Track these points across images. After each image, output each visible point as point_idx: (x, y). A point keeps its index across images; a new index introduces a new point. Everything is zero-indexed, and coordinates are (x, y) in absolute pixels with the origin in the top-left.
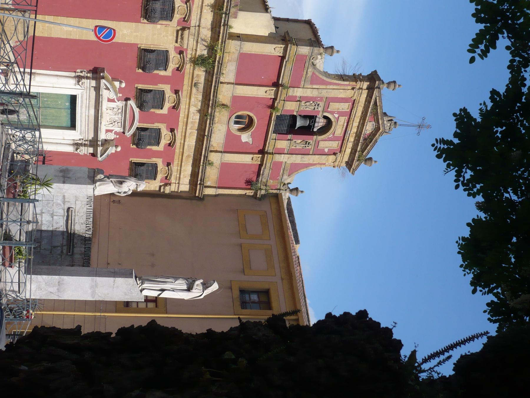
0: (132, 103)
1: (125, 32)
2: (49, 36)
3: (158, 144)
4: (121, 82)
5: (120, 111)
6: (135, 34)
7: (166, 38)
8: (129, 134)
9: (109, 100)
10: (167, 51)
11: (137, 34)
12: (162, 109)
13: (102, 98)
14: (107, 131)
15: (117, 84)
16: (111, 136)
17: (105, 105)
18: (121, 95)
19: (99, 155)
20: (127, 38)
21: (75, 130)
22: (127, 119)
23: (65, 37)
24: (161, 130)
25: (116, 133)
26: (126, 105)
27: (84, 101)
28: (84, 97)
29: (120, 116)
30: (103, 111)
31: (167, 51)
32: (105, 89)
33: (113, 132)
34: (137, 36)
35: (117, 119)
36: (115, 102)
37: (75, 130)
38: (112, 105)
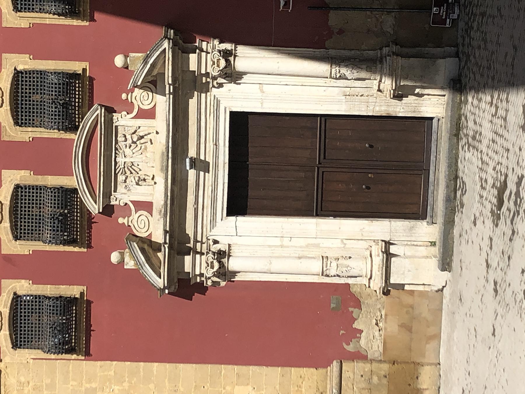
0: (94, 207)
1: (116, 388)
2: (287, 369)
3: (18, 75)
4: (122, 262)
5: (121, 178)
6: (94, 385)
7: (22, 379)
8: (96, 113)
9: (146, 206)
10: (16, 345)
11: (88, 386)
12: (17, 187)
13: (165, 225)
14: (149, 114)
15: (130, 264)
16: (141, 98)
17: (157, 193)
18: (121, 220)
19: (169, 55)
20: (112, 373)
21: (232, 114)
22: (103, 159)
23: (251, 367)
24: (11, 121)
25: (128, 107)
26: (107, 195)
27: (208, 202)
28: (208, 211)
29: (121, 160)
30: (163, 175)
31: (16, 345)
32: (157, 247)
33: (134, 113)
34: (89, 381)
35: (128, 151)
36: (131, 201)
37: (232, 114)
38: (141, 193)
